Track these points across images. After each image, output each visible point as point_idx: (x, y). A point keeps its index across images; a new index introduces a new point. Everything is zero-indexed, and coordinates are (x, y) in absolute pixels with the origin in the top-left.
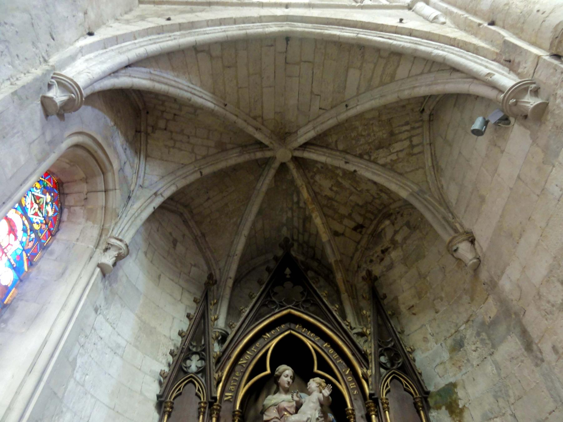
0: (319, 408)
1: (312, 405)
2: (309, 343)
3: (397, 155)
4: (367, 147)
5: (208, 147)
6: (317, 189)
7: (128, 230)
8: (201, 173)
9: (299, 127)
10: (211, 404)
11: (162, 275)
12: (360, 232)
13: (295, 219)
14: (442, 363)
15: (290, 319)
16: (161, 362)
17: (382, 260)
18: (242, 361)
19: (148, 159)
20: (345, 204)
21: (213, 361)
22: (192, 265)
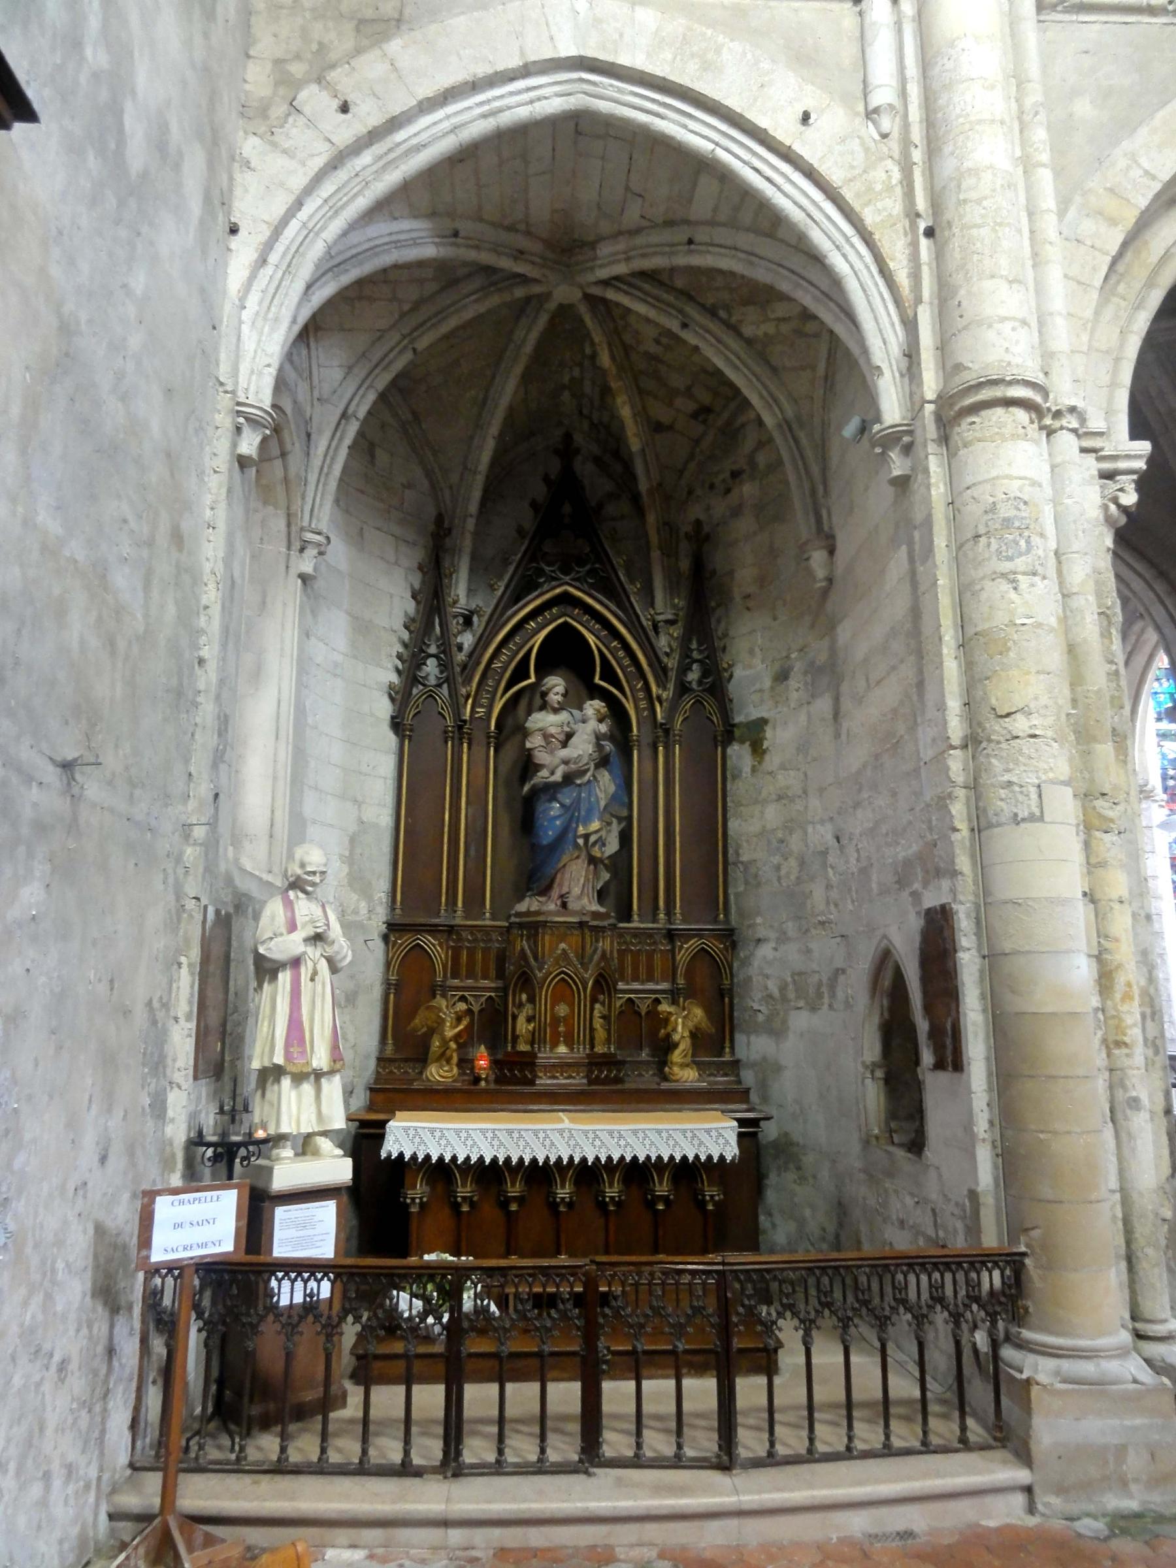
0: (594, 740)
2: (591, 639)
3: (777, 326)
5: (421, 282)
6: (628, 338)
7: (321, 505)
8: (414, 350)
9: (600, 239)
10: (460, 728)
11: (365, 527)
12: (704, 422)
14: (761, 691)
15: (565, 599)
16: (386, 669)
17: (728, 491)
18: (497, 665)
19: (319, 334)
21: (458, 669)
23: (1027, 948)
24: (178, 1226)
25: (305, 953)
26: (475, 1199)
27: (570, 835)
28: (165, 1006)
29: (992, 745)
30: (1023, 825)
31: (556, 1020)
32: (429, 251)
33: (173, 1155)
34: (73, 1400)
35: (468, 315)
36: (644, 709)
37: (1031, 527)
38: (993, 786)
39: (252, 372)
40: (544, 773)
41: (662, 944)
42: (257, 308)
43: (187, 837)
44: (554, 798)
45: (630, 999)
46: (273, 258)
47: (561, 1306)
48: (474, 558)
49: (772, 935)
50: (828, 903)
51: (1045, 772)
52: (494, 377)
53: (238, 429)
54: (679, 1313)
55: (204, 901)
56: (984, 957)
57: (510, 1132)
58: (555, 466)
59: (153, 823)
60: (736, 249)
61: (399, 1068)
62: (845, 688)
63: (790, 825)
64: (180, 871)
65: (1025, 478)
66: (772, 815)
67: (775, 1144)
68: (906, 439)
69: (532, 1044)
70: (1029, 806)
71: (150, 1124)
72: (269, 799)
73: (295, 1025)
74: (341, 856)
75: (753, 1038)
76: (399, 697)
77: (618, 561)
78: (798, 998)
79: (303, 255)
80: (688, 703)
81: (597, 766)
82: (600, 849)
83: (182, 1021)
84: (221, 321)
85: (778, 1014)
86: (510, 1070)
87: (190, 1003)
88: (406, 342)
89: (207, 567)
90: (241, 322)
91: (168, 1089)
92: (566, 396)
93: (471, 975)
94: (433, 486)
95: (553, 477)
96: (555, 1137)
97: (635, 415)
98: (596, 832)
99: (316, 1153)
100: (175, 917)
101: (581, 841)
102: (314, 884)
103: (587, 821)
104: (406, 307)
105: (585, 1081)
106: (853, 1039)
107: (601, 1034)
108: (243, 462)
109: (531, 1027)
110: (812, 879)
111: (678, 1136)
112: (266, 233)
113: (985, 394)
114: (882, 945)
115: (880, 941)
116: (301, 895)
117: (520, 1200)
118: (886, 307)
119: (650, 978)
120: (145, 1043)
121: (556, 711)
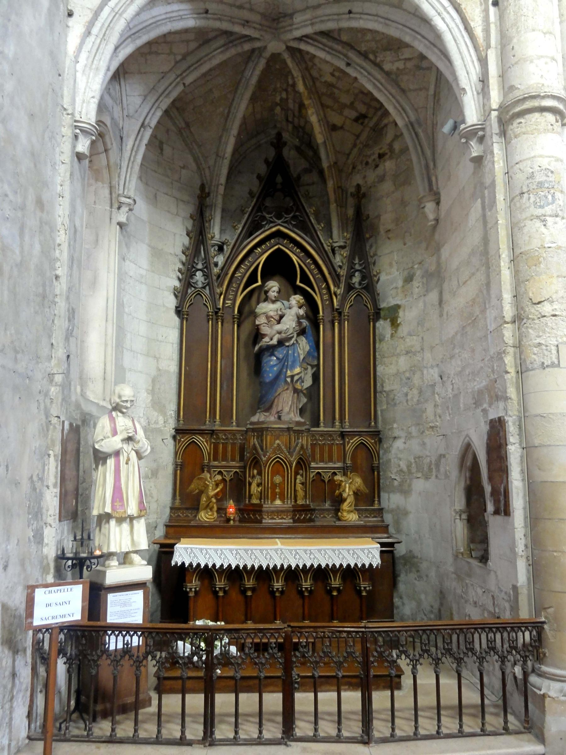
0: (296, 319)
1: (291, 317)
2: (294, 258)
3: (405, 64)
4: (373, 45)
5: (188, 42)
6: (315, 73)
7: (130, 181)
8: (184, 84)
10: (216, 313)
12: (362, 124)
13: (290, 101)
14: (396, 288)
15: (279, 234)
16: (172, 278)
17: (377, 166)
18: (238, 275)
19: (126, 76)
20: (348, 91)
21: (215, 278)
23: (549, 443)
25: (122, 448)
26: (227, 589)
27: (283, 376)
28: (41, 479)
29: (530, 321)
30: (547, 370)
31: (274, 486)
32: (190, 23)
33: (48, 564)
35: (215, 62)
36: (326, 300)
37: (555, 187)
38: (530, 345)
39: (84, 101)
40: (266, 339)
41: (338, 441)
42: (85, 62)
43: (51, 381)
44: (272, 354)
45: (318, 473)
46: (95, 31)
47: (271, 651)
48: (223, 210)
49: (403, 434)
50: (435, 416)
51: (561, 338)
52: (233, 100)
53: (76, 137)
54: (339, 655)
55: (62, 418)
56: (523, 449)
57: (246, 551)
58: (271, 153)
59: (30, 374)
60: (377, 15)
61: (183, 513)
62: (446, 286)
63: (413, 369)
64: (48, 401)
65: (553, 157)
66: (403, 363)
67: (403, 557)
68: (481, 133)
69: (260, 499)
70: (551, 358)
71: (34, 547)
72: (103, 358)
73: (117, 490)
74: (147, 390)
75: (392, 495)
76: (180, 295)
77: (310, 211)
78: (418, 471)
79: (113, 28)
80: (352, 296)
81: (298, 335)
82: (300, 384)
83: (51, 487)
84: (64, 72)
85: (406, 481)
86: (248, 515)
87: (56, 477)
88: (179, 79)
89: (59, 220)
90: (76, 71)
91: (44, 527)
92: (278, 110)
93: (224, 459)
94: (199, 168)
95: (270, 160)
97: (319, 121)
98: (298, 374)
99: (131, 563)
101: (289, 380)
102: (127, 408)
103: (293, 367)
104: (179, 58)
105: (291, 521)
106: (449, 496)
107: (300, 493)
108: (79, 157)
109: (259, 489)
110: (426, 401)
111: (345, 554)
113: (528, 105)
114: (466, 441)
115: (465, 438)
116: (119, 414)
117: (253, 590)
118: (469, 51)
119: (331, 460)
120: (29, 501)
121: (273, 302)
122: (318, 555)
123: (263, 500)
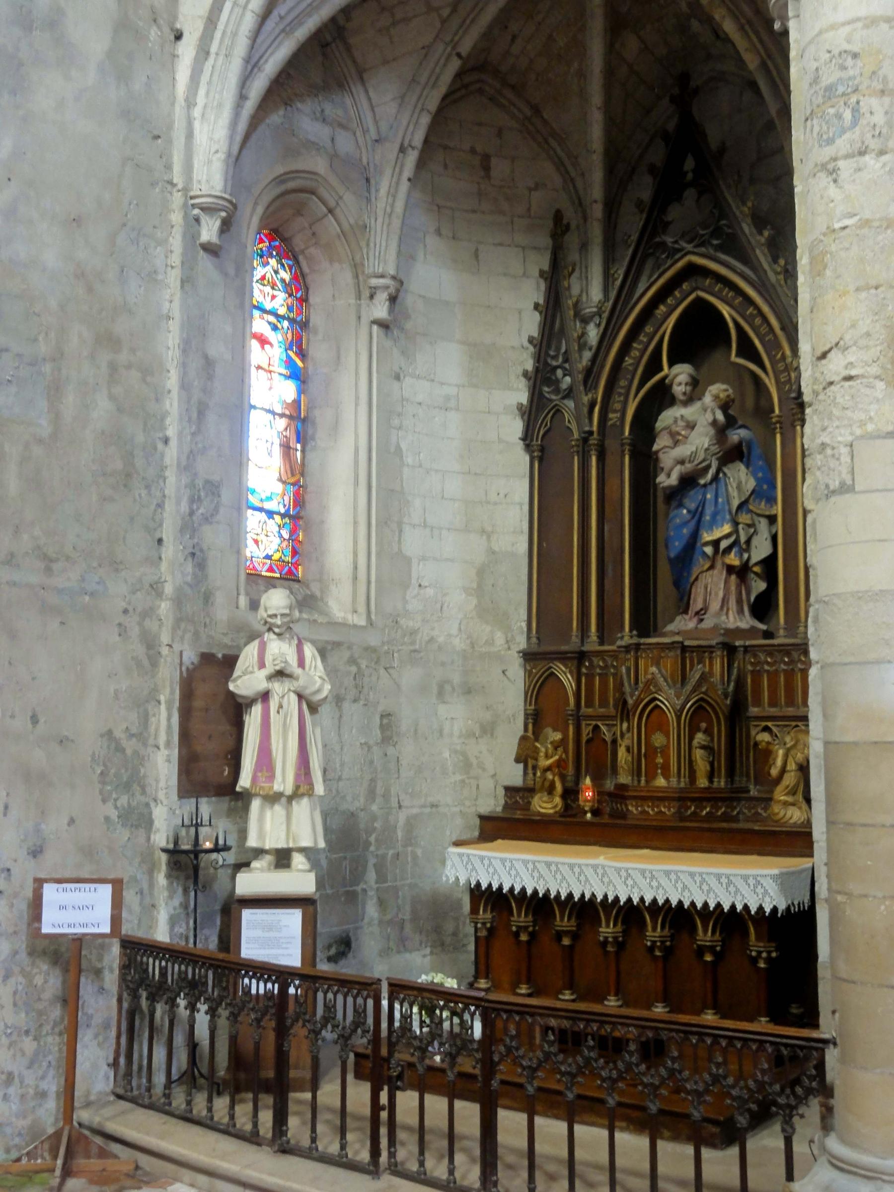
2: (725, 311)
7: (387, 246)
8: (459, 55)
15: (692, 271)
16: (518, 389)
18: (628, 361)
21: (581, 377)
22: (530, 190)
24: (63, 908)
28: (141, 735)
30: (833, 499)
31: (652, 751)
34: (6, 1027)
37: (862, 87)
43: (160, 594)
44: (681, 505)
46: (214, 48)
53: (197, 220)
55: (177, 647)
57: (548, 865)
61: (522, 798)
65: (858, 19)
70: (840, 473)
74: (466, 590)
91: (152, 804)
92: (695, 25)
96: (589, 872)
97: (742, 28)
100: (146, 662)
101: (709, 550)
104: (446, 12)
108: (210, 249)
112: (200, 25)
122: (664, 881)
123: (643, 779)
